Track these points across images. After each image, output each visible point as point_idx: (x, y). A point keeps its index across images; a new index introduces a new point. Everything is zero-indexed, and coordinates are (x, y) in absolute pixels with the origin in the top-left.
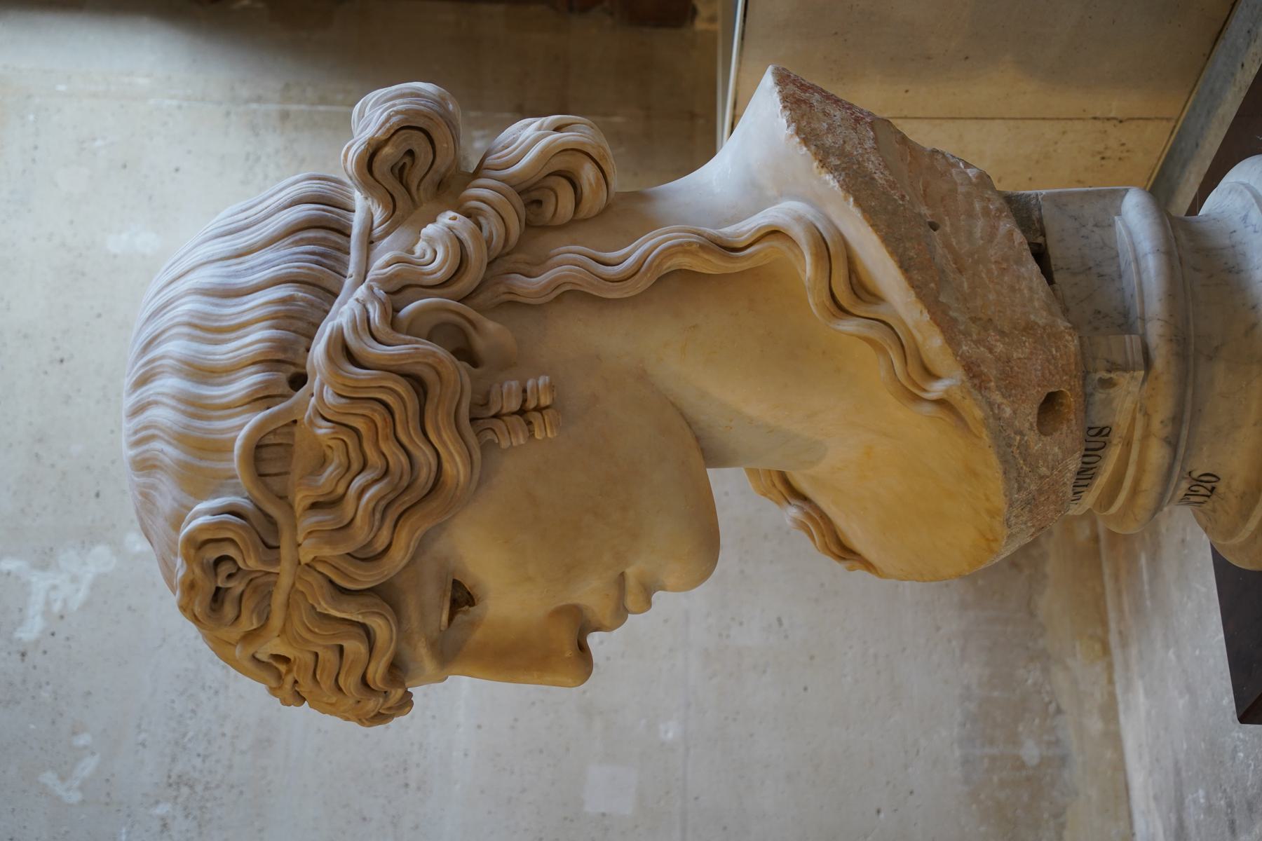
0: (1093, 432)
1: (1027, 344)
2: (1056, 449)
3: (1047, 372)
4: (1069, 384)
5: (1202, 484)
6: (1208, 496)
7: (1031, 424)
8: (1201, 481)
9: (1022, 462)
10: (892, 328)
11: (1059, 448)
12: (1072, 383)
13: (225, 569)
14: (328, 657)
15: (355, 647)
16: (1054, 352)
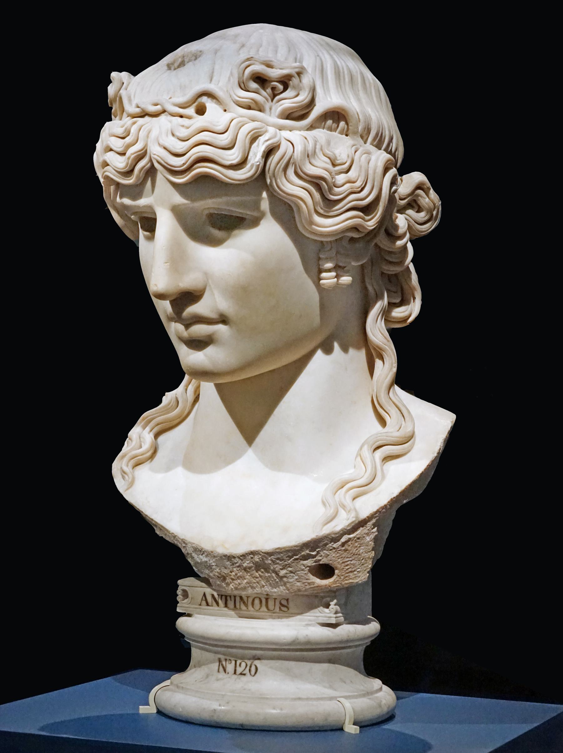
0: (284, 602)
1: (366, 554)
2: (296, 577)
3: (348, 567)
4: (337, 581)
5: (248, 668)
6: (235, 673)
7: (320, 560)
8: (251, 667)
9: (297, 557)
10: (373, 480)
11: (297, 579)
12: (337, 582)
13: (281, 87)
14: (224, 140)
15: (233, 156)
16: (358, 570)
